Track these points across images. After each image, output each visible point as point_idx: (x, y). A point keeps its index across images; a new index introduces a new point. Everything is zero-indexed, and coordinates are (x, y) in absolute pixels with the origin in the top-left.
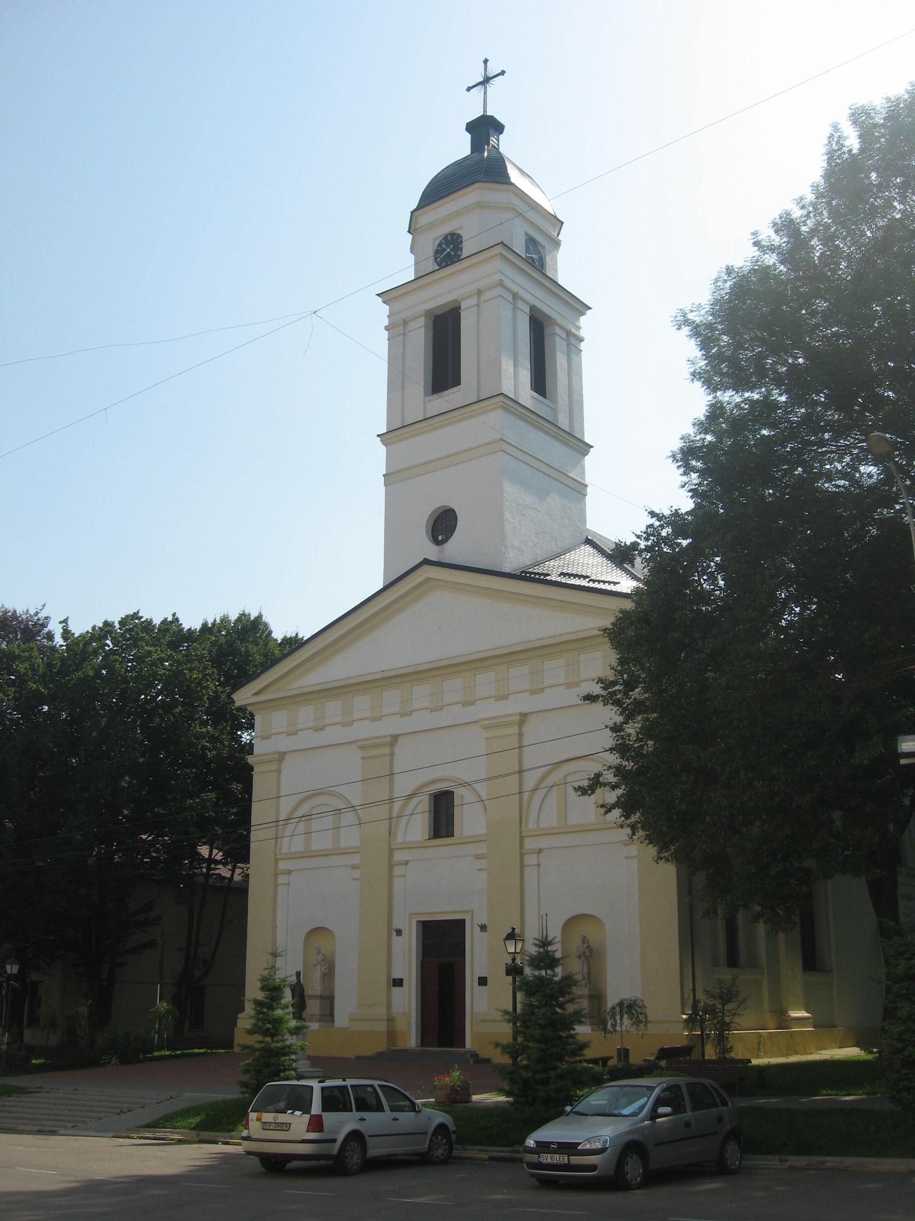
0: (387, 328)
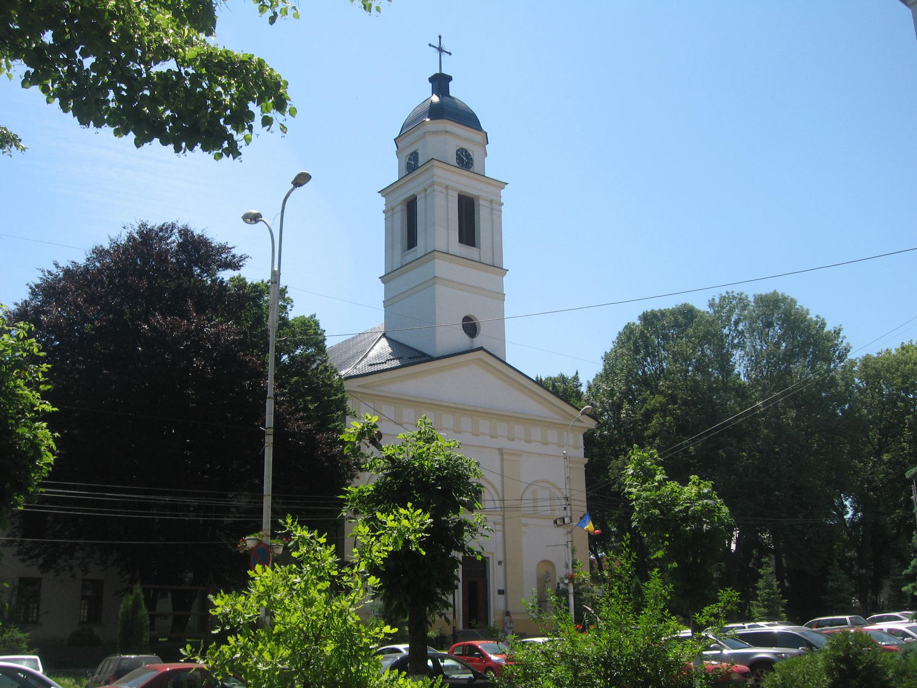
0: (384, 212)
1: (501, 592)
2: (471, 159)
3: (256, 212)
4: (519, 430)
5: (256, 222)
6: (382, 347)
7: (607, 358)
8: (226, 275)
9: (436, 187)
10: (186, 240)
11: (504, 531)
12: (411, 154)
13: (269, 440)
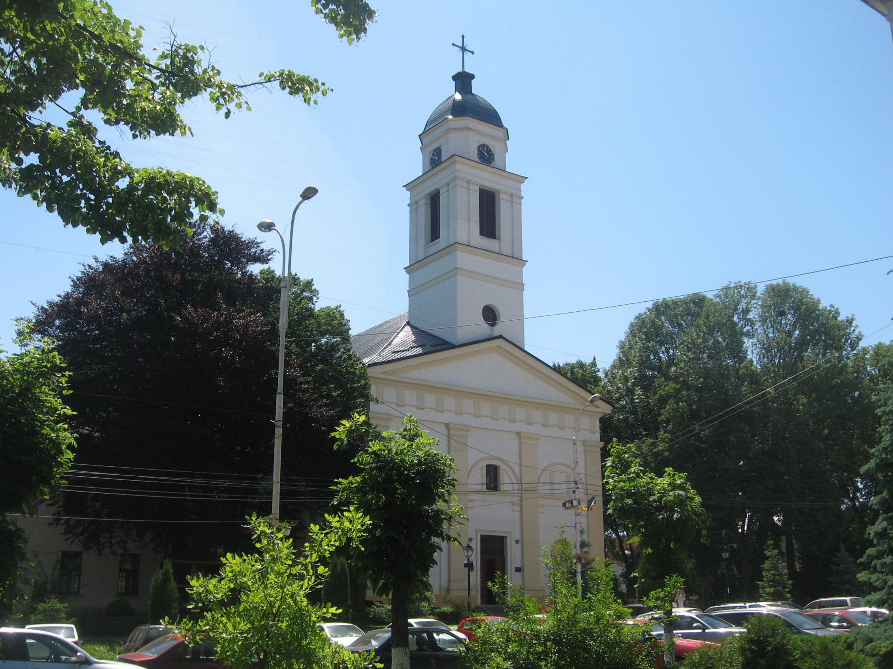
1: (518, 570)
2: (492, 155)
3: (269, 221)
4: (537, 415)
5: (270, 230)
6: (406, 335)
7: (622, 346)
8: (255, 269)
9: (458, 182)
10: (217, 236)
11: (521, 512)
12: (435, 150)
13: (279, 431)
